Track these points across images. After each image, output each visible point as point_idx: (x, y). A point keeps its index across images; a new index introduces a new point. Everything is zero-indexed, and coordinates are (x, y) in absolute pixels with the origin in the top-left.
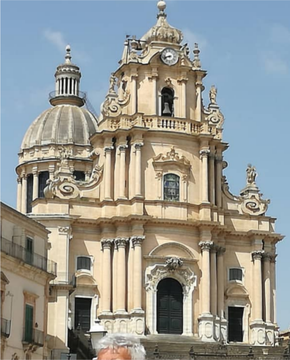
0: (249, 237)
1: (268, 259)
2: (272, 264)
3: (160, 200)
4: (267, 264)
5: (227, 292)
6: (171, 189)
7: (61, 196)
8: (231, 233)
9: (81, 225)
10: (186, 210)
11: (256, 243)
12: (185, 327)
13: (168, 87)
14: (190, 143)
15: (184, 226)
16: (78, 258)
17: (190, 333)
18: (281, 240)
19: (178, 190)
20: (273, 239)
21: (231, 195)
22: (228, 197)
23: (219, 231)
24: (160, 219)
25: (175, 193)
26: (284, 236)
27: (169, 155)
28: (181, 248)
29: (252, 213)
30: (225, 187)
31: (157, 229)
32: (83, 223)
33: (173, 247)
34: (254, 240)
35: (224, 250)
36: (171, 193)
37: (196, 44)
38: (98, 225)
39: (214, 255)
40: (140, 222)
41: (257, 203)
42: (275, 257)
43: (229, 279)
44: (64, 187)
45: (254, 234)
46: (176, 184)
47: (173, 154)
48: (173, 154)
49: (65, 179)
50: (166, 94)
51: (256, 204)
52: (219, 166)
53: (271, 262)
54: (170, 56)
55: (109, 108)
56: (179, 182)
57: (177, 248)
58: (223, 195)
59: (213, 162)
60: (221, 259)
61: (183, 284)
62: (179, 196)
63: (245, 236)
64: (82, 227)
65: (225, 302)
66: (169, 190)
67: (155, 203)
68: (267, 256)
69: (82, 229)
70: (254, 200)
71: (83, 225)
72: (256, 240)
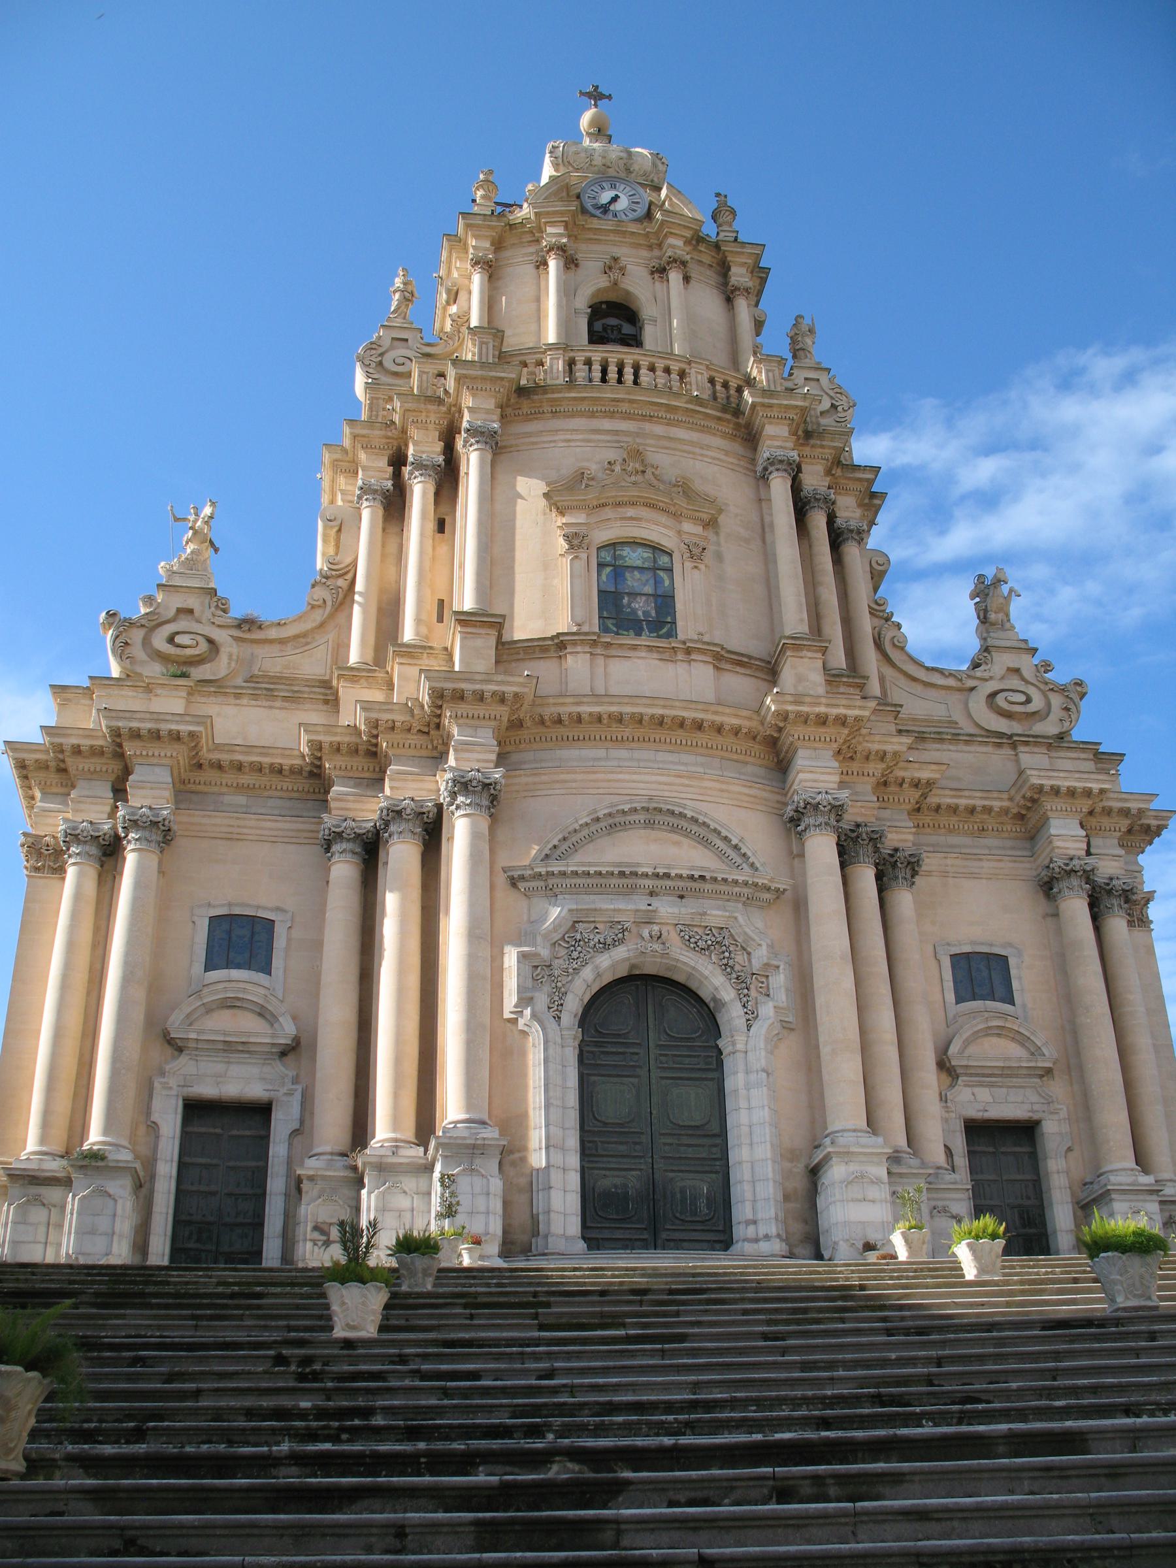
0: (1021, 817)
1: (1115, 902)
2: (1138, 933)
3: (585, 629)
4: (1117, 925)
5: (953, 1049)
6: (633, 595)
7: (154, 670)
8: (933, 800)
9: (230, 778)
10: (710, 670)
11: (1053, 831)
12: (741, 1211)
13: (612, 297)
14: (717, 441)
15: (702, 738)
16: (212, 919)
17: (767, 1237)
18: (1158, 831)
19: (665, 602)
20: (1124, 824)
21: (920, 664)
22: (915, 679)
23: (876, 768)
24: (579, 699)
25: (653, 614)
26: (1164, 817)
27: (618, 468)
28: (695, 828)
29: (1015, 727)
30: (888, 635)
31: (571, 754)
32: (239, 767)
33: (649, 824)
34: (1044, 821)
35: (913, 866)
36: (634, 612)
37: (718, 195)
38: (312, 774)
39: (866, 877)
40: (481, 710)
41: (1033, 692)
42: (1148, 901)
43: (951, 997)
44: (171, 640)
45: (1040, 789)
46: (657, 582)
47: (633, 465)
48: (633, 465)
49: (180, 611)
50: (613, 321)
51: (1029, 700)
52: (851, 551)
53: (1130, 924)
54: (615, 199)
55: (380, 363)
56: (670, 570)
57: (674, 829)
58: (889, 672)
59: (818, 521)
60: (904, 900)
61: (714, 999)
62: (674, 623)
63: (1005, 811)
64: (240, 788)
65: (943, 1098)
66: (625, 601)
67: (559, 645)
68: (1109, 892)
69: (241, 800)
70: (1015, 683)
71: (246, 779)
72: (1054, 822)
